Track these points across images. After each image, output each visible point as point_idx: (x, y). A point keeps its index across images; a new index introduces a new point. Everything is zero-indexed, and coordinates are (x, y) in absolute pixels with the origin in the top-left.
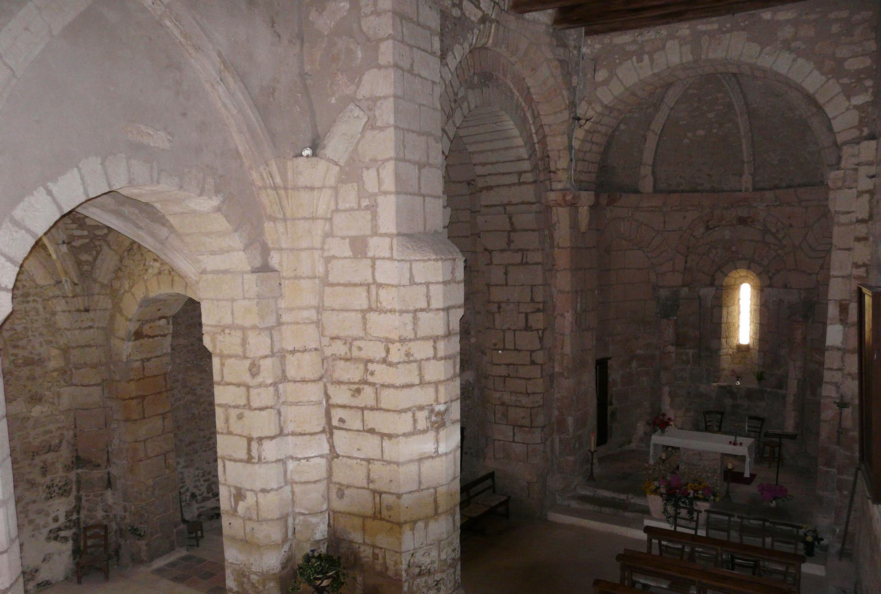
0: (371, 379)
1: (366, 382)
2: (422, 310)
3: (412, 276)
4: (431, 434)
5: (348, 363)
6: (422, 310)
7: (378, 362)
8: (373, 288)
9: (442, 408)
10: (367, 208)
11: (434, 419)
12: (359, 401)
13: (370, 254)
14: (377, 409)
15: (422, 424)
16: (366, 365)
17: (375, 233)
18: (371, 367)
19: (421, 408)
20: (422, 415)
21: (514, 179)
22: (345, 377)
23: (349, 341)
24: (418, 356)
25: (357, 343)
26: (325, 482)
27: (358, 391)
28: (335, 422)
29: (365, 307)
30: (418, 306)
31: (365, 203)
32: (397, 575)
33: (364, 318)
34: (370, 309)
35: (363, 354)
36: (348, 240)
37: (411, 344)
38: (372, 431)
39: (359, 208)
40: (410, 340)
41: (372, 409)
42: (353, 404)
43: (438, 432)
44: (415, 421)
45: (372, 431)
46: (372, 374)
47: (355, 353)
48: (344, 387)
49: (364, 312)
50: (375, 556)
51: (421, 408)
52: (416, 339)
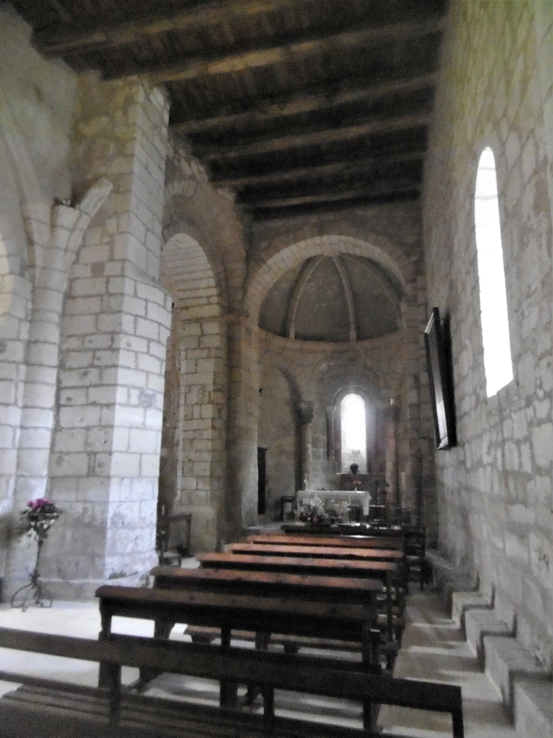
0: (97, 363)
1: (92, 366)
2: (141, 317)
3: (135, 292)
4: (140, 411)
5: (79, 354)
6: (141, 317)
7: (105, 349)
8: (106, 298)
9: (150, 392)
10: (107, 243)
11: (143, 399)
12: (86, 382)
13: (106, 273)
14: (101, 385)
15: (134, 400)
16: (94, 353)
17: (112, 259)
18: (98, 354)
19: (135, 388)
20: (135, 394)
21: (204, 301)
22: (75, 365)
23: (82, 337)
24: (135, 347)
25: (88, 338)
26: (47, 452)
27: (85, 374)
28: (63, 401)
29: (98, 311)
30: (139, 313)
31: (106, 240)
32: (102, 523)
33: (97, 318)
34: (102, 312)
35: (92, 346)
36: (90, 266)
37: (131, 338)
38: (94, 404)
39: (101, 243)
40: (131, 335)
41: (96, 386)
42: (81, 385)
43: (146, 411)
44: (129, 396)
45: (94, 404)
46: (99, 359)
47: (87, 345)
48: (76, 372)
49: (97, 314)
50: (85, 510)
51: (135, 388)
52: (135, 335)
